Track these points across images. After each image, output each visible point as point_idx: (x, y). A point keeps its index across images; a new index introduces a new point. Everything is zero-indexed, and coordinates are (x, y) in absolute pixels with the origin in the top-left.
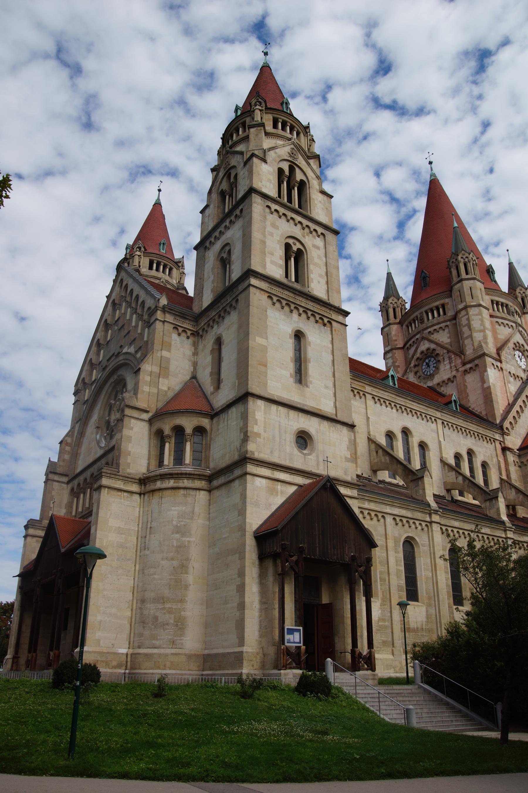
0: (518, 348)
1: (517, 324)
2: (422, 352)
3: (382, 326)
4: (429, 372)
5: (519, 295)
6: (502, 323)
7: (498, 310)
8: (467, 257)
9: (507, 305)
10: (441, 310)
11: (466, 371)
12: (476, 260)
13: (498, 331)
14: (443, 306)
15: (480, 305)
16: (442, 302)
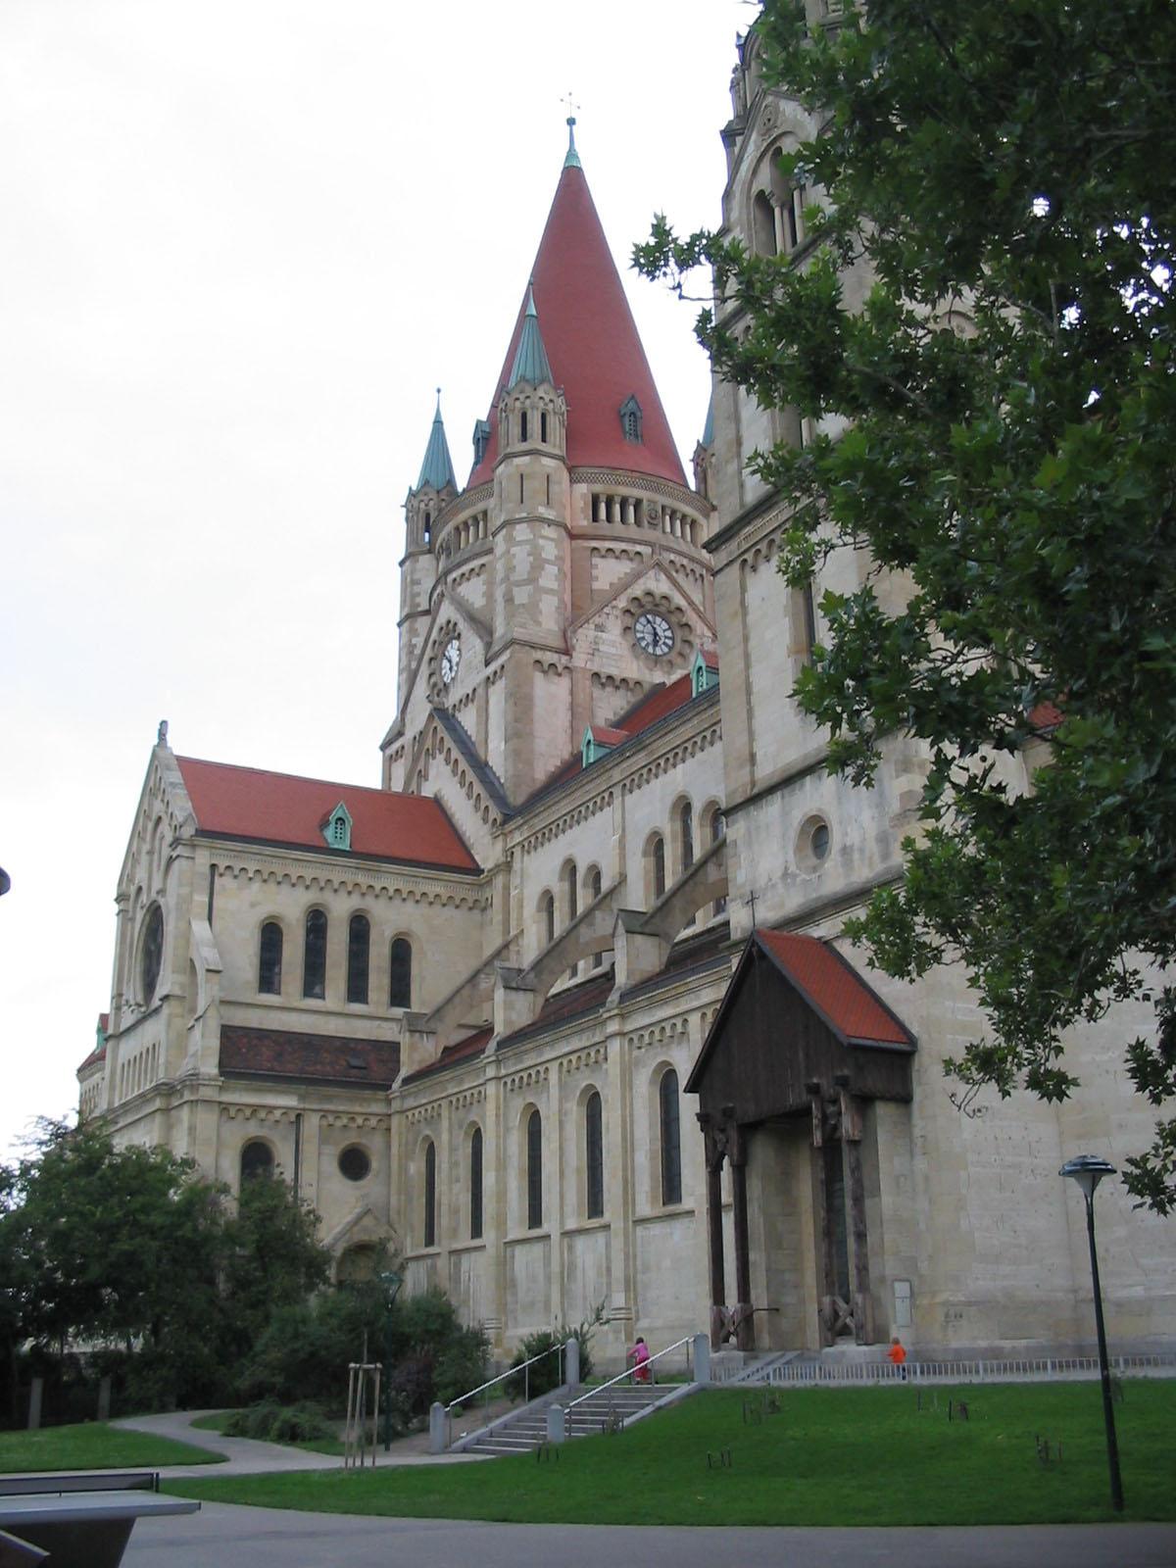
3: (401, 555)
6: (609, 550)
7: (609, 518)
13: (595, 572)
14: (485, 513)
16: (481, 506)
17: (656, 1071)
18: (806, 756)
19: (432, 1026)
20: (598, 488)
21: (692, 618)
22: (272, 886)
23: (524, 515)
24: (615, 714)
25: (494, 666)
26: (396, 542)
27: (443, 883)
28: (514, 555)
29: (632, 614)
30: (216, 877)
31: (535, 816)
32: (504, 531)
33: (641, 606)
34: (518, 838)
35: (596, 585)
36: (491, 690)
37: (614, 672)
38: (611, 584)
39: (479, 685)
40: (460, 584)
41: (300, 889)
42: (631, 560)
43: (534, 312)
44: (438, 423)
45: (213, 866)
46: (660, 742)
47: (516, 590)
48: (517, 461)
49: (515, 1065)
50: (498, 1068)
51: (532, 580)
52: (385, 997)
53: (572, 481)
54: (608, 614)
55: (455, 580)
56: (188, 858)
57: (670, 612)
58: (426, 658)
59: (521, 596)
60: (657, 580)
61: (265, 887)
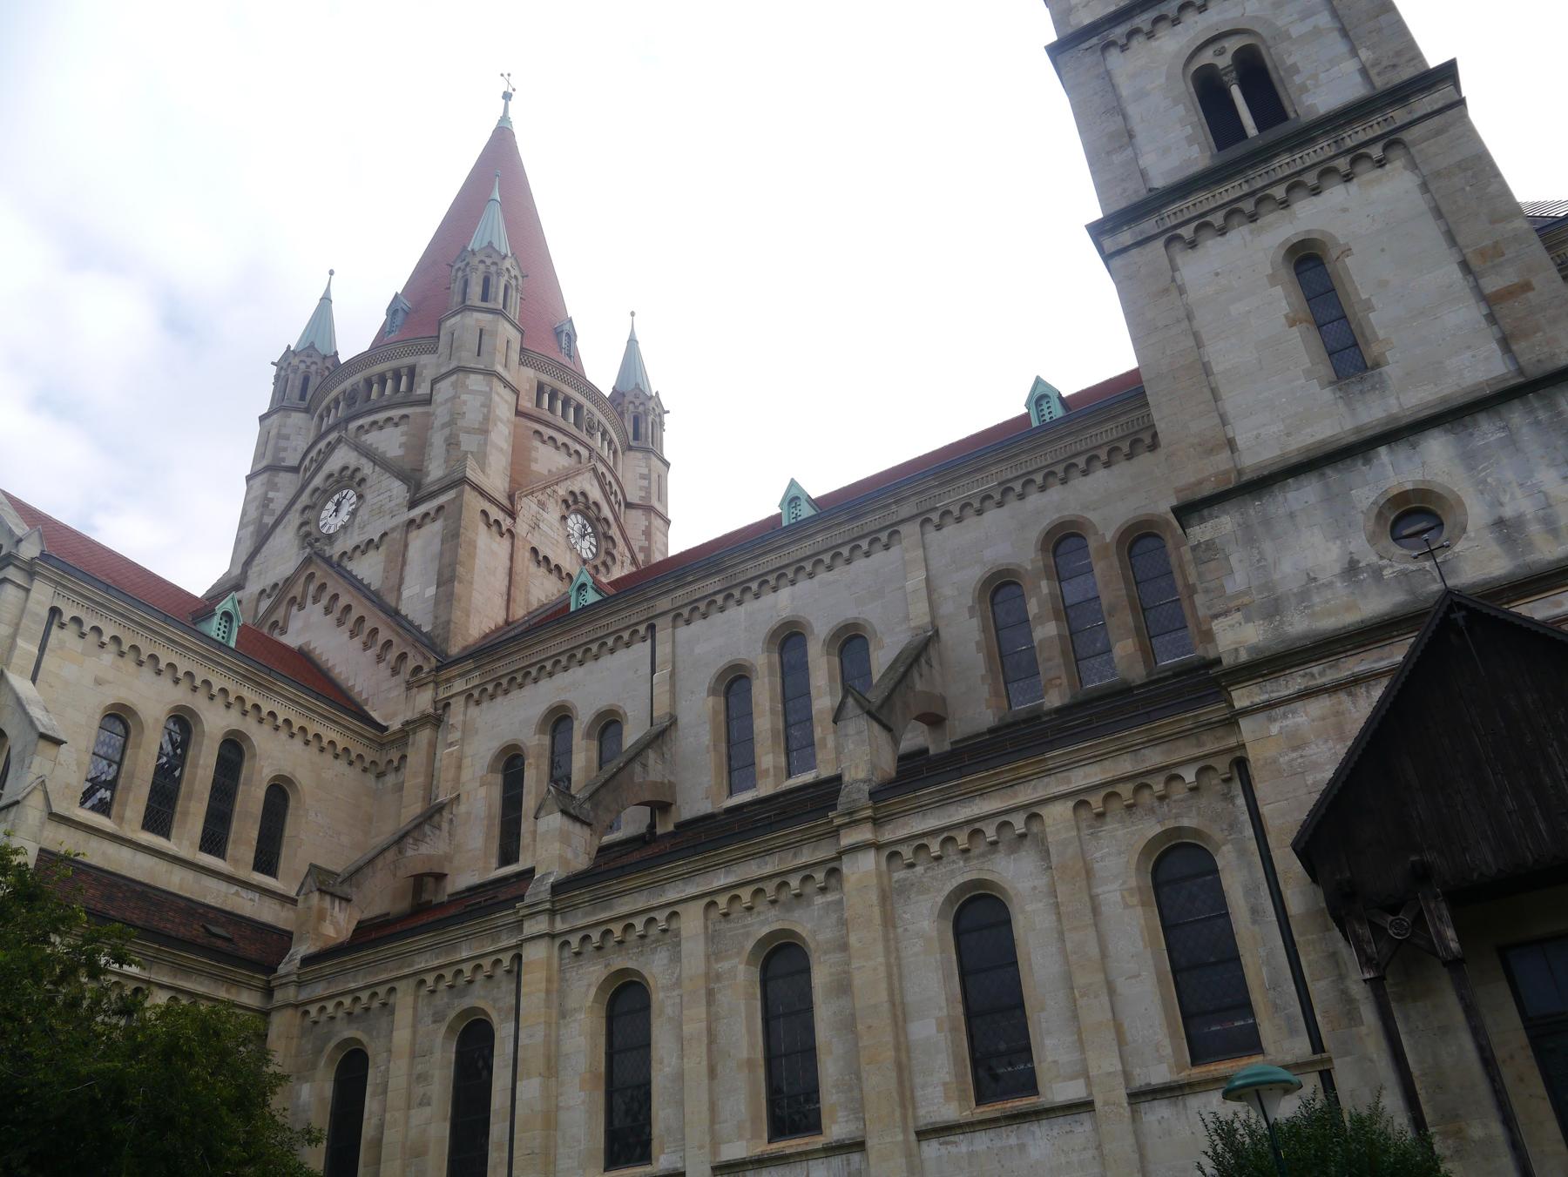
0: (581, 506)
1: (594, 454)
2: (331, 475)
3: (265, 410)
4: (333, 527)
5: (631, 407)
6: (551, 438)
8: (494, 263)
9: (578, 408)
10: (404, 379)
11: (412, 521)
12: (520, 278)
13: (534, 454)
14: (412, 372)
15: (490, 374)
17: (950, 899)
18: (1358, 430)
19: (346, 890)
20: (545, 378)
21: (614, 532)
22: (129, 663)
23: (482, 367)
24: (547, 596)
25: (417, 512)
26: (262, 399)
27: (341, 730)
28: (465, 403)
29: (568, 507)
30: (55, 628)
31: (499, 659)
32: (454, 377)
33: (576, 501)
34: (459, 685)
35: (535, 467)
36: (414, 534)
37: (551, 556)
38: (549, 471)
39: (393, 529)
40: (367, 432)
41: (165, 682)
42: (570, 455)
43: (499, 199)
44: (326, 300)
45: (55, 612)
46: (750, 564)
47: (463, 437)
48: (476, 315)
49: (586, 915)
50: (552, 922)
51: (484, 432)
52: (249, 855)
53: (521, 363)
54: (549, 496)
55: (361, 427)
56: (19, 586)
57: (598, 519)
58: (299, 506)
59: (468, 443)
60: (592, 485)
61: (120, 662)
